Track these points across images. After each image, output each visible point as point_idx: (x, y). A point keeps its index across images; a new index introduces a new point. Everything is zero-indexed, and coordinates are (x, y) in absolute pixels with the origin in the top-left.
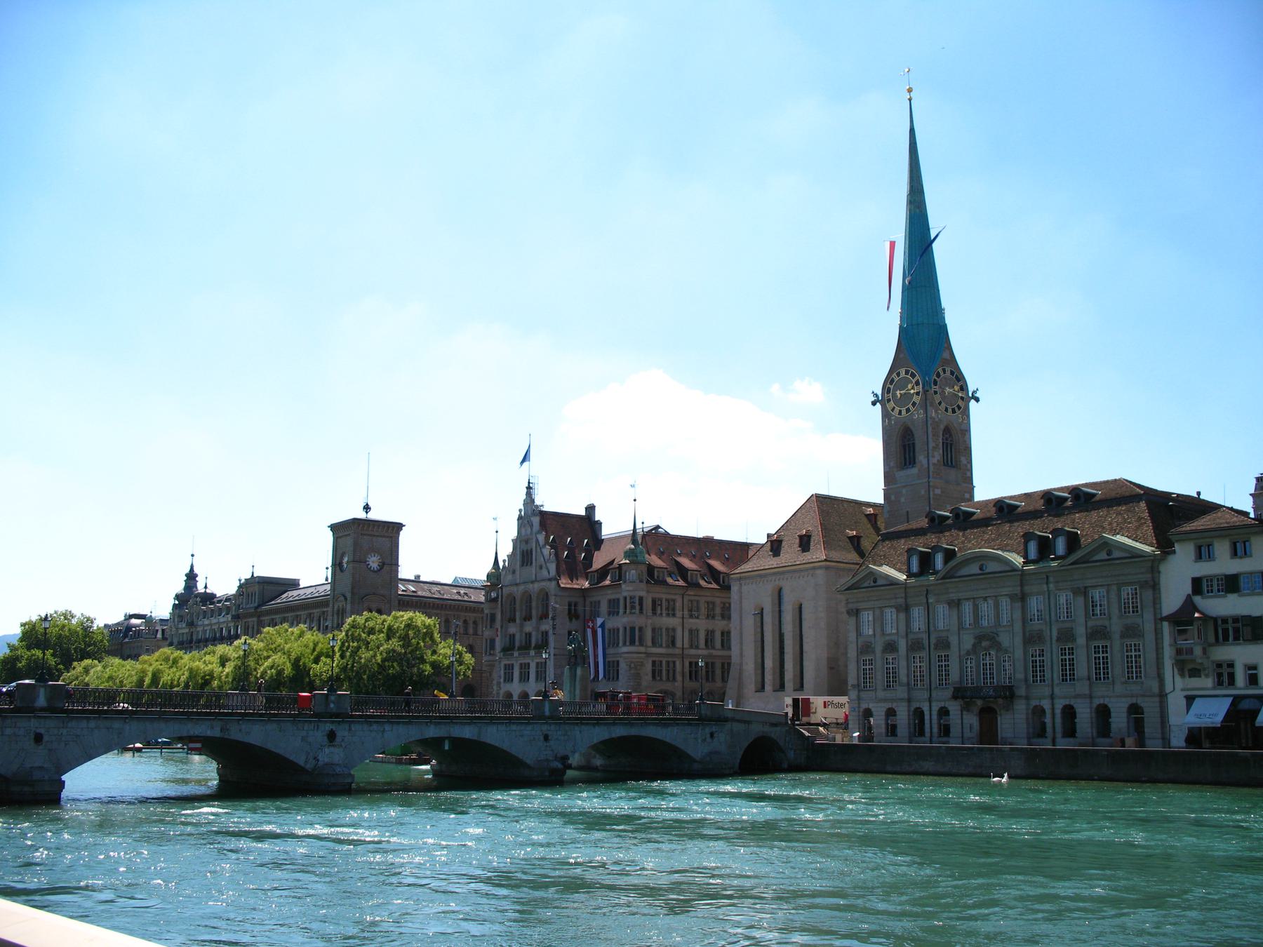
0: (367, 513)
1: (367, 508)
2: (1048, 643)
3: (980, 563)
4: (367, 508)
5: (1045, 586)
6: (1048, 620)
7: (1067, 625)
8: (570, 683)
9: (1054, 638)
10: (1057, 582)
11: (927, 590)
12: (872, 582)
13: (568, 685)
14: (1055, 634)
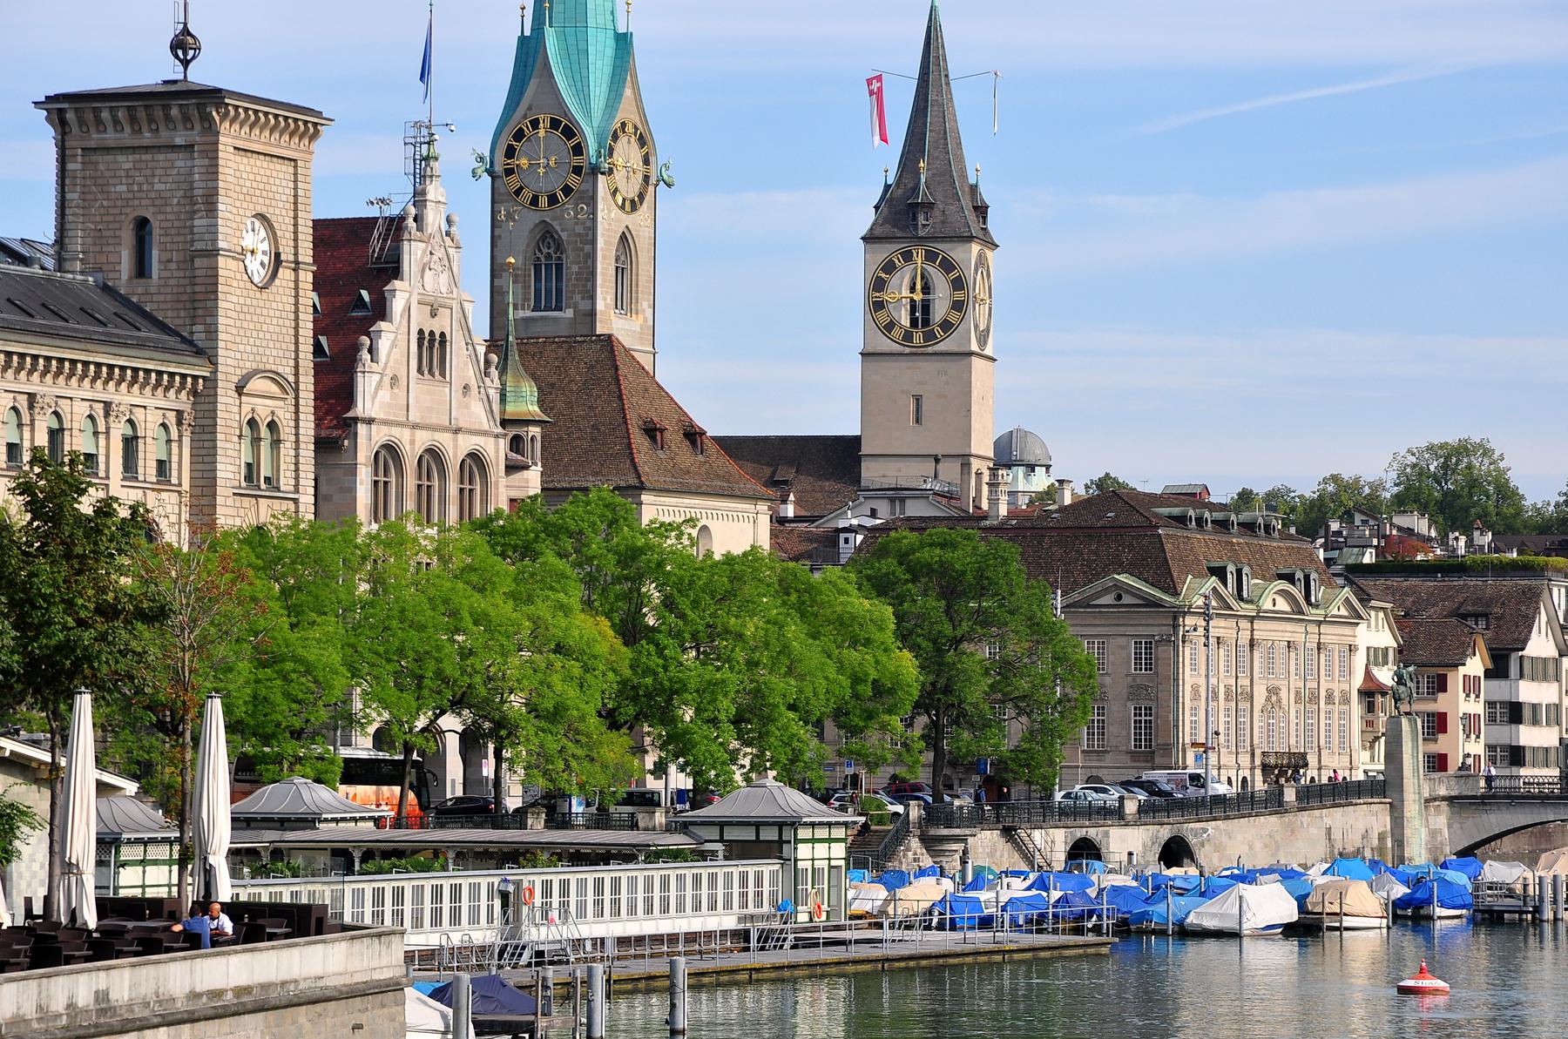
0: (186, 63)
1: (183, 45)
4: (183, 45)
8: (1412, 741)
13: (1410, 745)
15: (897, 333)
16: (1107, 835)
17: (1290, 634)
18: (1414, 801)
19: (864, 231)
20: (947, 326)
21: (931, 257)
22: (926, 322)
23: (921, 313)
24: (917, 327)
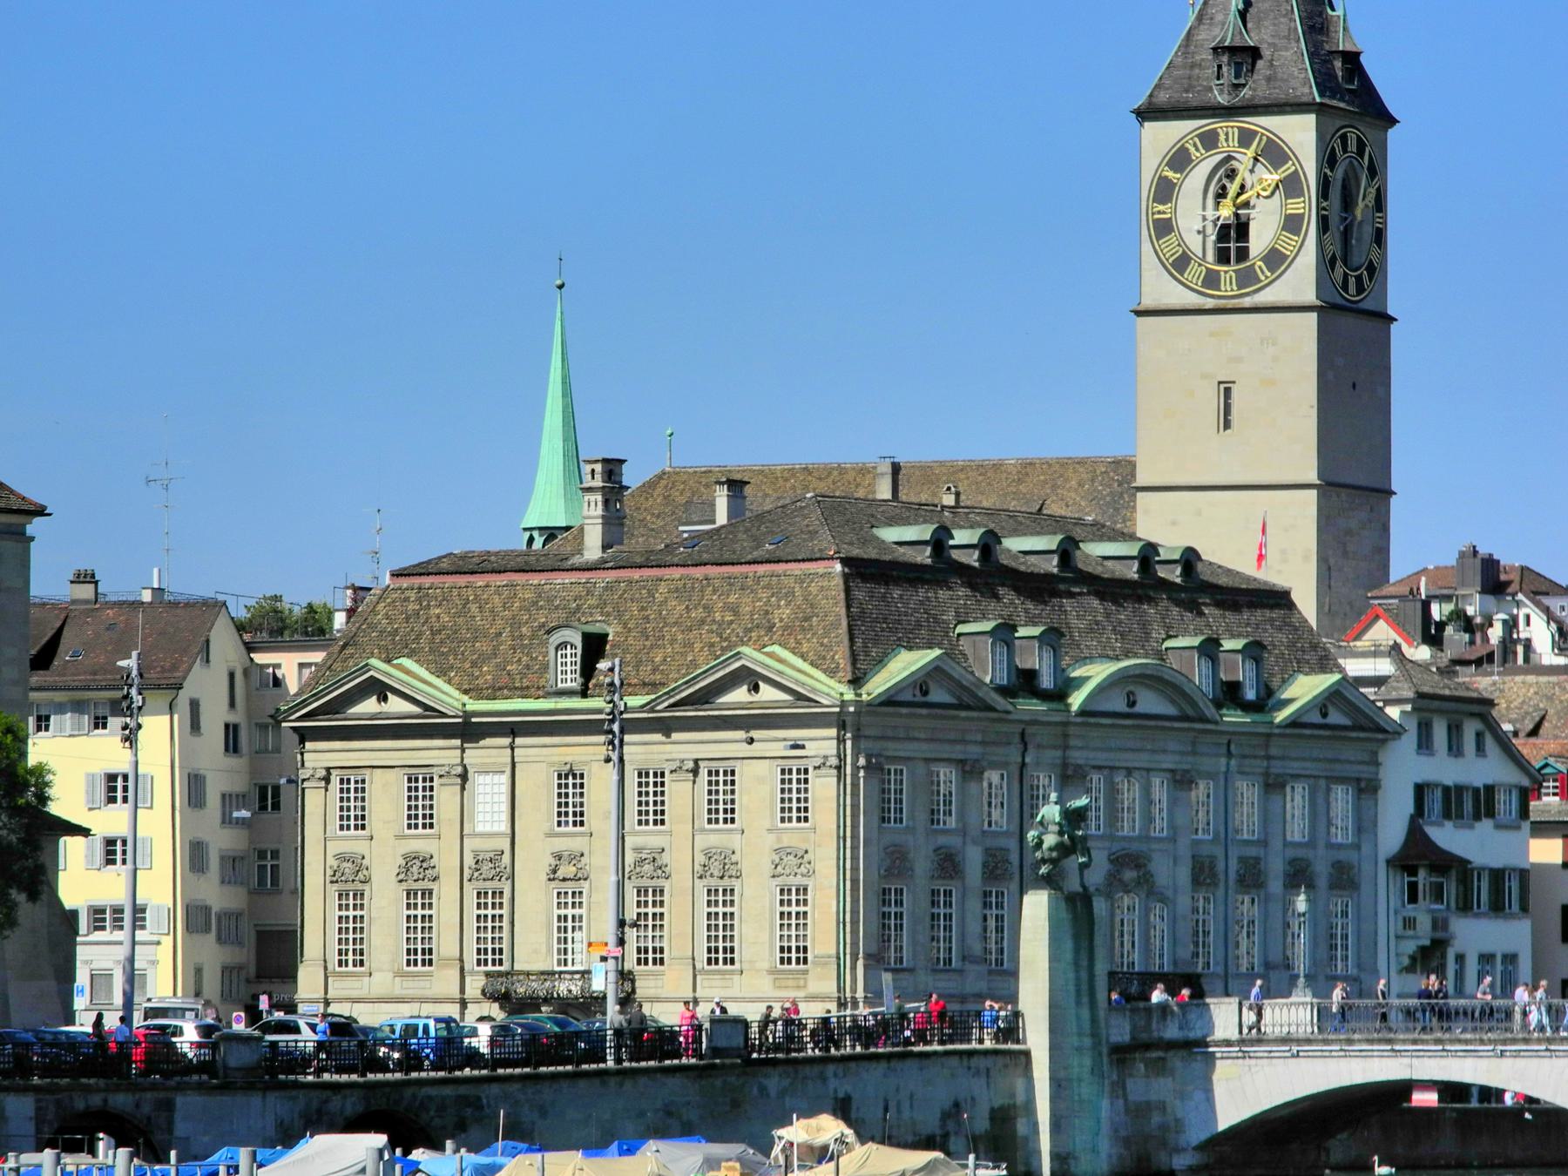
2: (1222, 885)
3: (1128, 689)
5: (1223, 761)
6: (1223, 836)
7: (1252, 852)
8: (1076, 937)
9: (1232, 875)
10: (1244, 757)
11: (1023, 734)
12: (918, 692)
14: (1234, 865)
15: (1194, 273)
16: (168, 1106)
17: (1177, 758)
18: (1079, 1049)
19: (1140, 101)
20: (1275, 259)
21: (1246, 138)
22: (1243, 254)
23: (1233, 235)
24: (1227, 262)
